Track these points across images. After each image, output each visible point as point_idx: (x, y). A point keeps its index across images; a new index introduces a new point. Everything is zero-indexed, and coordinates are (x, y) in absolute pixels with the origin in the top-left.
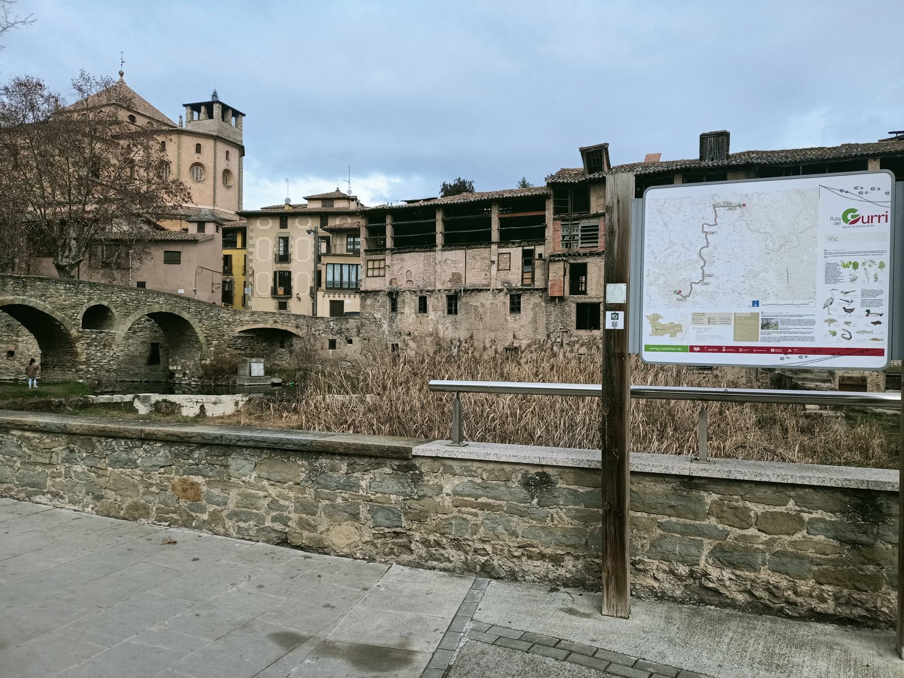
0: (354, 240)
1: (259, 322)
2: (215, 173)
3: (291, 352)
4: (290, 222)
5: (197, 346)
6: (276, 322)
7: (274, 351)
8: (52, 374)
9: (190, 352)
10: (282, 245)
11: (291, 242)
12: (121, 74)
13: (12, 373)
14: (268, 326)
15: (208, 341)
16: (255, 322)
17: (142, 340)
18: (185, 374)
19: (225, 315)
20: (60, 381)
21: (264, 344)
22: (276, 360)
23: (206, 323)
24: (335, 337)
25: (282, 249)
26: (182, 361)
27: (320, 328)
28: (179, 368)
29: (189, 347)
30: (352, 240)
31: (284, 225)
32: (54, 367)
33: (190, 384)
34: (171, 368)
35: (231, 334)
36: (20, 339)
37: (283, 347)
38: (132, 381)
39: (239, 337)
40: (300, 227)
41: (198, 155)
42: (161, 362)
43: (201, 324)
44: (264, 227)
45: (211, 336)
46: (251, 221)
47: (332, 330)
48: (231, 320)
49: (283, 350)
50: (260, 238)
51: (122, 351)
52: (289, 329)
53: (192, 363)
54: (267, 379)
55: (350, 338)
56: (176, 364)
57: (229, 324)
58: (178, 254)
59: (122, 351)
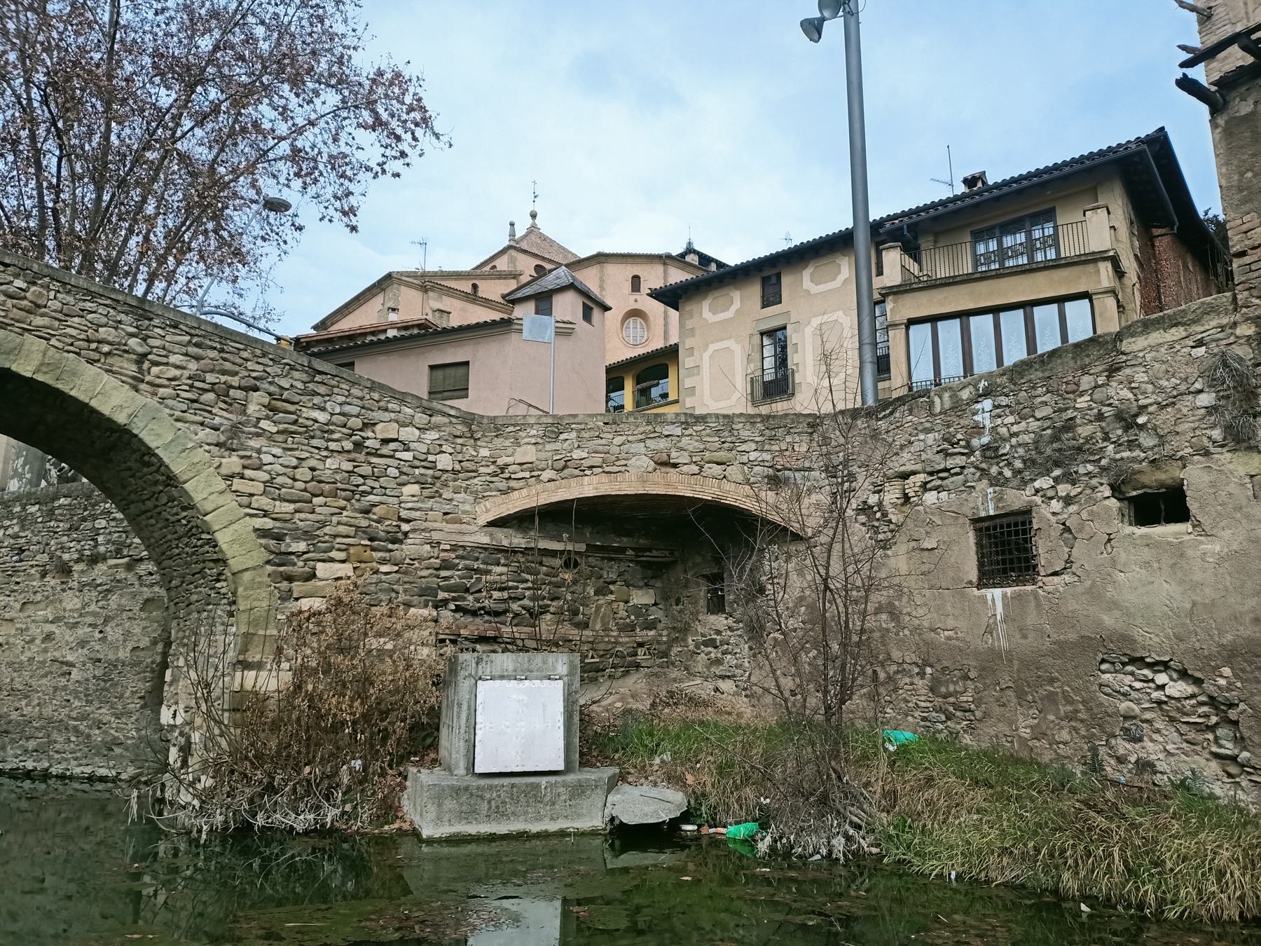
0: (1000, 243)
1: (584, 470)
2: (666, 325)
3: (755, 631)
4: (786, 281)
6: (666, 464)
7: (686, 630)
10: (769, 351)
11: (792, 336)
12: (534, 216)
14: (627, 485)
15: (283, 558)
16: (564, 467)
17: (147, 593)
19: (408, 433)
21: (641, 598)
22: (692, 675)
23: (274, 457)
24: (1017, 499)
25: (769, 363)
27: (905, 461)
30: (993, 245)
31: (771, 297)
35: (446, 533)
37: (717, 605)
38: (91, 779)
39: (496, 552)
40: (814, 289)
41: (636, 296)
43: (232, 463)
44: (721, 316)
45: (307, 535)
46: (689, 307)
47: (991, 452)
48: (444, 461)
49: (720, 621)
50: (712, 347)
51: (82, 644)
52: (737, 495)
54: (579, 791)
55: (1153, 478)
57: (432, 483)
58: (461, 370)
59: (82, 644)
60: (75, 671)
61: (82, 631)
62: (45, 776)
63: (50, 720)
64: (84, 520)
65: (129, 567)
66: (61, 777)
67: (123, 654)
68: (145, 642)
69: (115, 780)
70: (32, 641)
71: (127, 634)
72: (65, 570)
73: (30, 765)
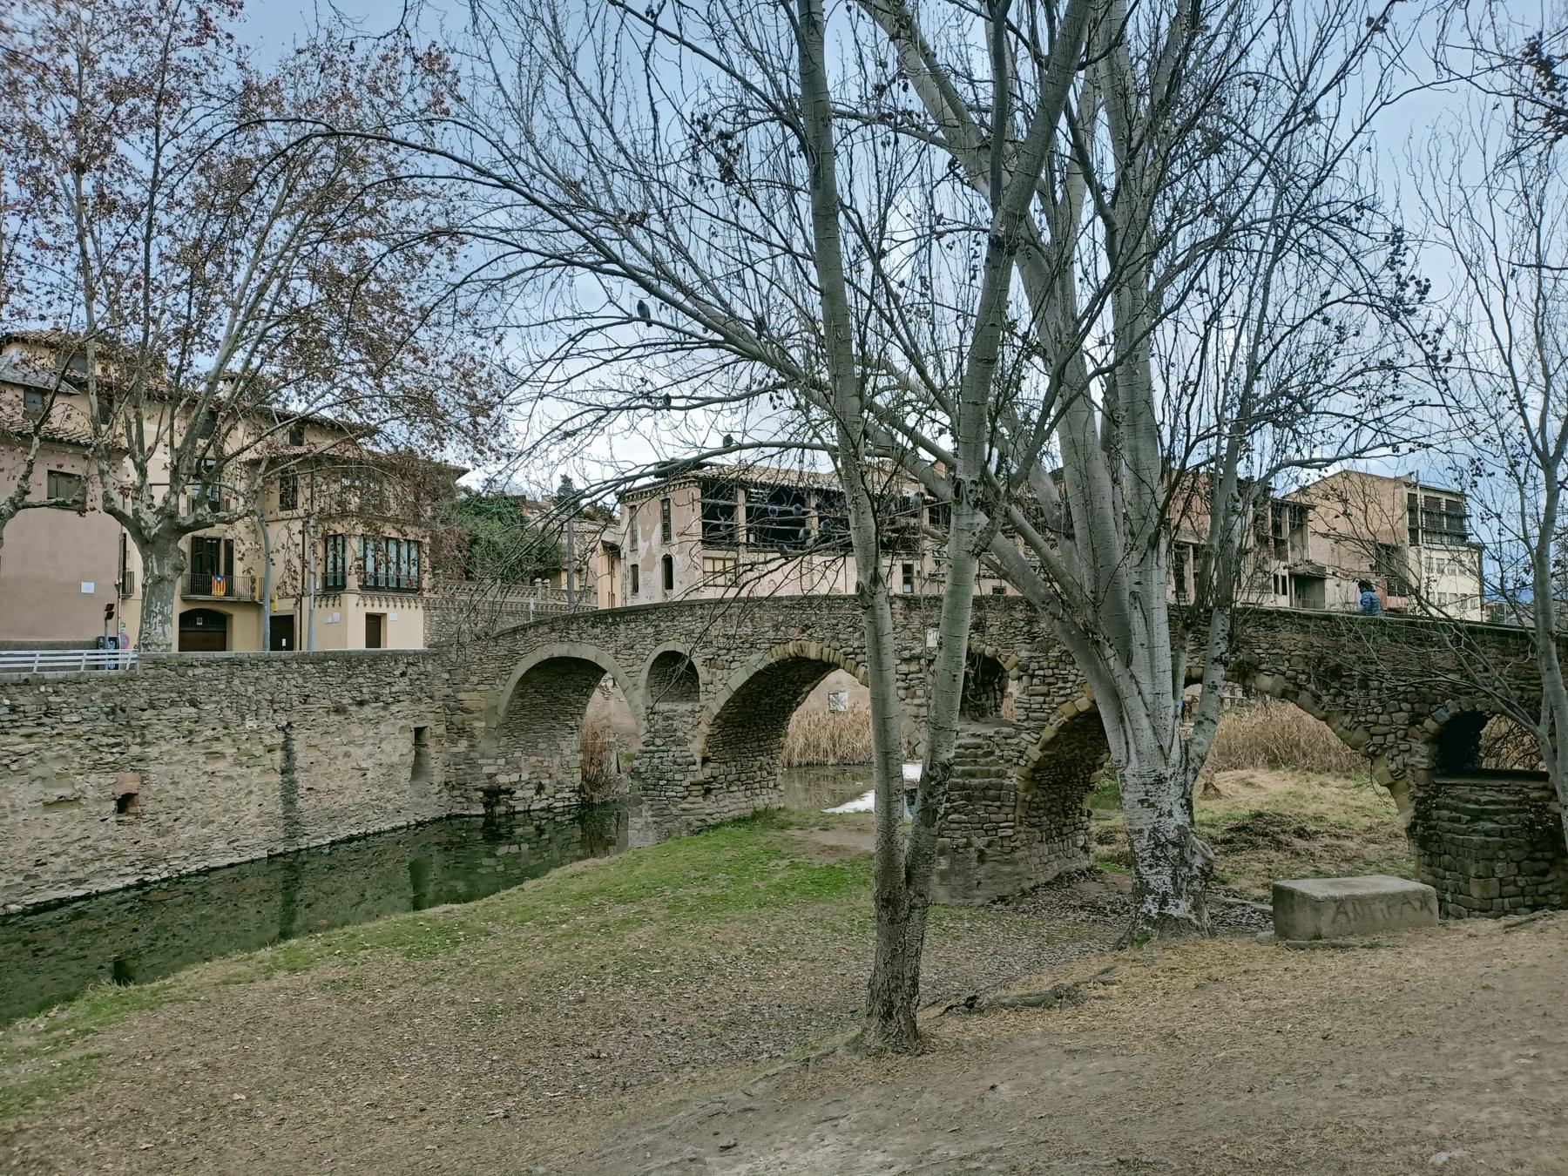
5: (572, 724)
8: (727, 802)
9: (550, 739)
13: (132, 864)
18: (540, 788)
20: (748, 813)
26: (533, 759)
28: (525, 777)
29: (553, 727)
32: (730, 784)
33: (549, 809)
34: (503, 780)
36: (152, 752)
42: (436, 772)
51: (371, 756)
53: (557, 760)
56: (519, 769)
59: (371, 756)
60: (370, 775)
61: (369, 748)
62: (366, 835)
63: (360, 804)
64: (349, 677)
65: (385, 708)
66: (375, 834)
67: (395, 759)
68: (405, 751)
69: (408, 827)
70: (336, 757)
71: (395, 748)
72: (340, 710)
73: (354, 832)
